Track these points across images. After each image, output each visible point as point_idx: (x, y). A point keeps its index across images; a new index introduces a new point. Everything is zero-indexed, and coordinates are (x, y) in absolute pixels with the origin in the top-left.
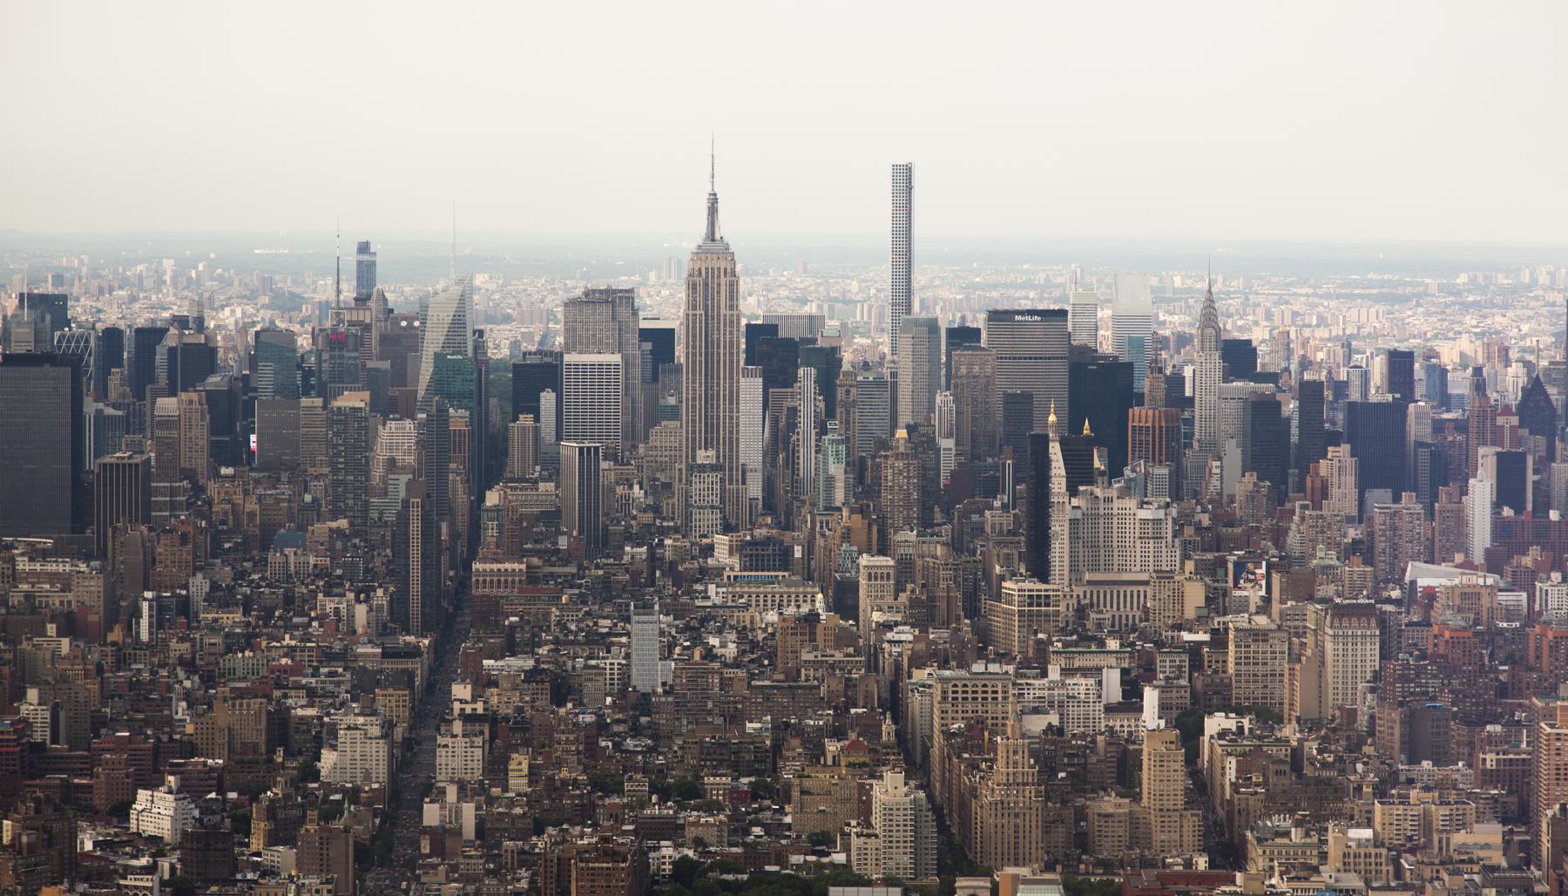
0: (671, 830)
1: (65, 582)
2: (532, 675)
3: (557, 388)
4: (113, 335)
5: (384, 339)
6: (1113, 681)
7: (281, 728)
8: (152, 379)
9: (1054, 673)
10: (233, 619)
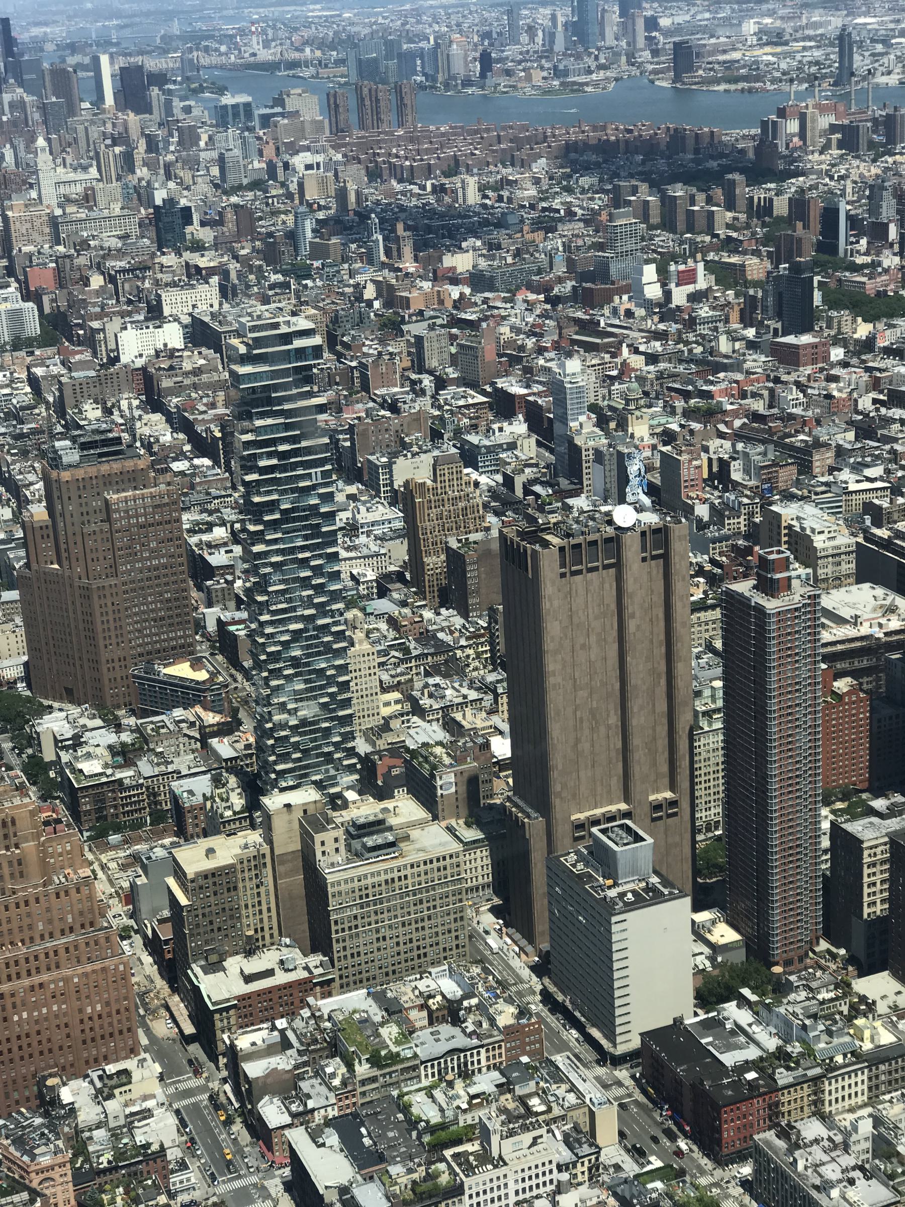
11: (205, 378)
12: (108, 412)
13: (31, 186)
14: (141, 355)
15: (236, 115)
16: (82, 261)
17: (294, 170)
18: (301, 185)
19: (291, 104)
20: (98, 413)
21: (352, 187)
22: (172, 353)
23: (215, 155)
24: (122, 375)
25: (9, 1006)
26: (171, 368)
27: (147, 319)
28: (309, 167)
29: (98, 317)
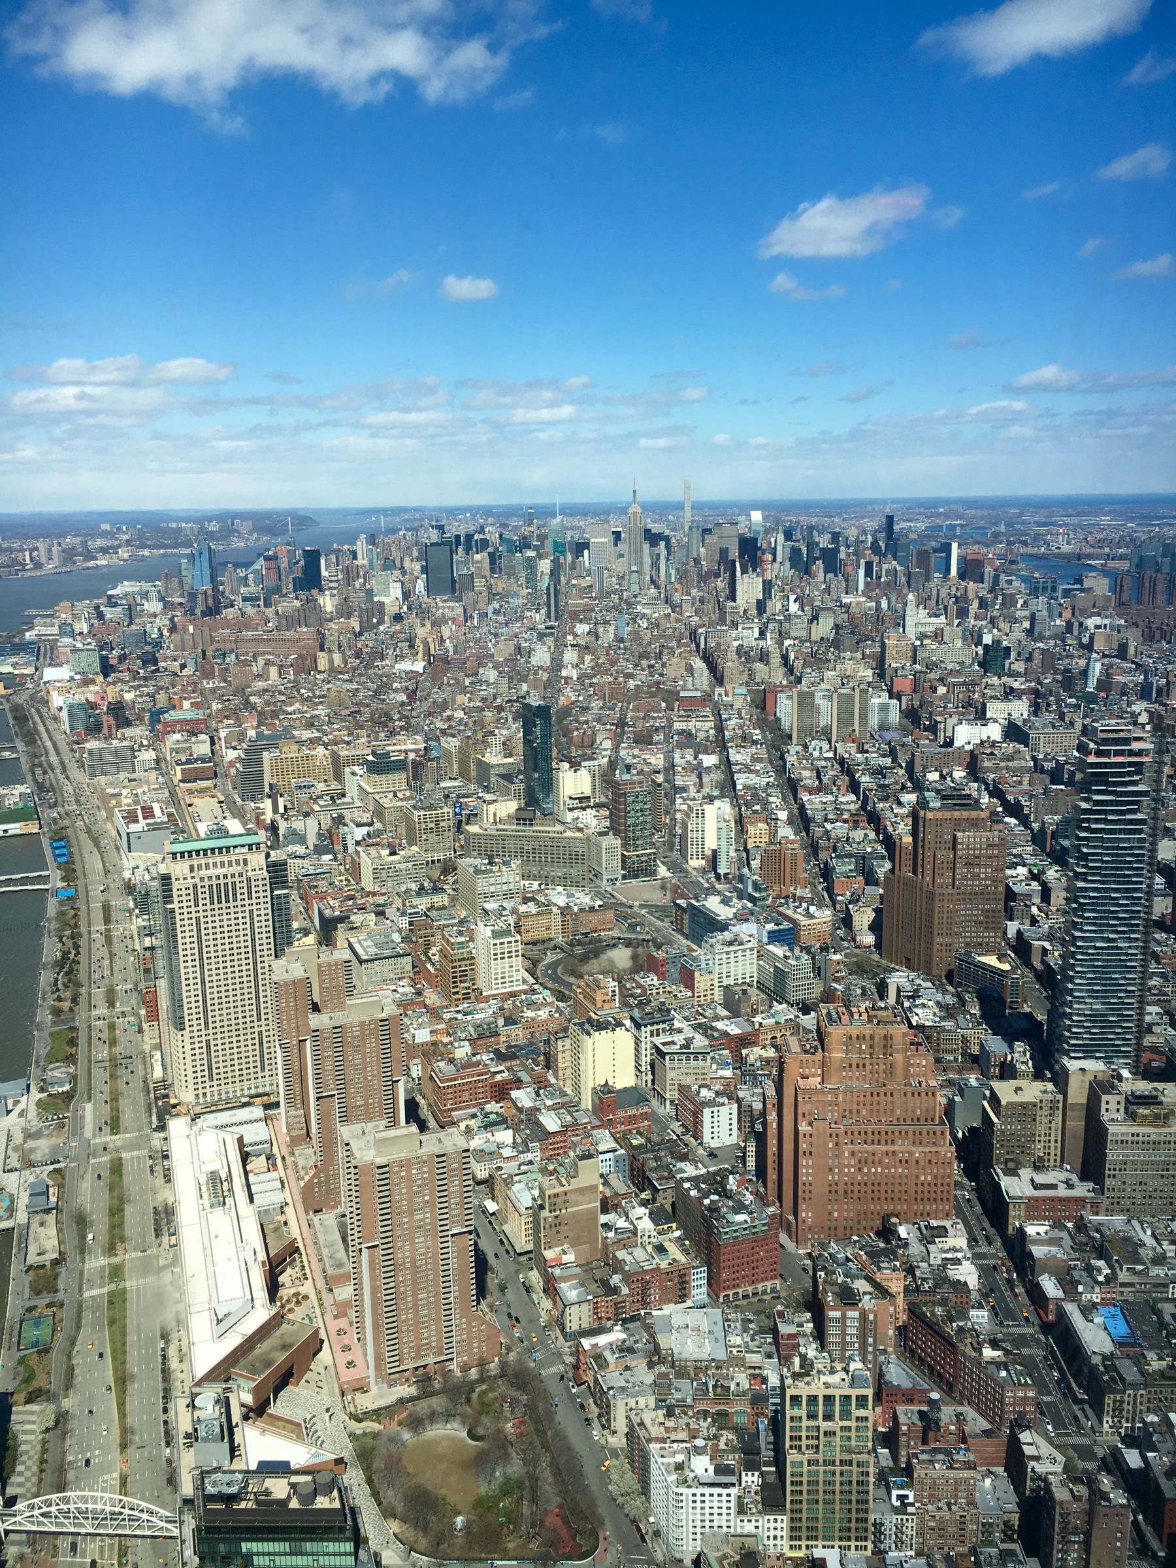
0: (631, 676)
1: (452, 608)
6: (756, 631)
7: (519, 649)
9: (740, 629)
10: (501, 618)
13: (899, 625)
15: (1045, 589)
16: (932, 676)
17: (1086, 628)
18: (1092, 638)
19: (1086, 585)
22: (993, 744)
23: (1027, 613)
24: (956, 755)
26: (992, 754)
27: (975, 719)
28: (1097, 627)
29: (940, 714)
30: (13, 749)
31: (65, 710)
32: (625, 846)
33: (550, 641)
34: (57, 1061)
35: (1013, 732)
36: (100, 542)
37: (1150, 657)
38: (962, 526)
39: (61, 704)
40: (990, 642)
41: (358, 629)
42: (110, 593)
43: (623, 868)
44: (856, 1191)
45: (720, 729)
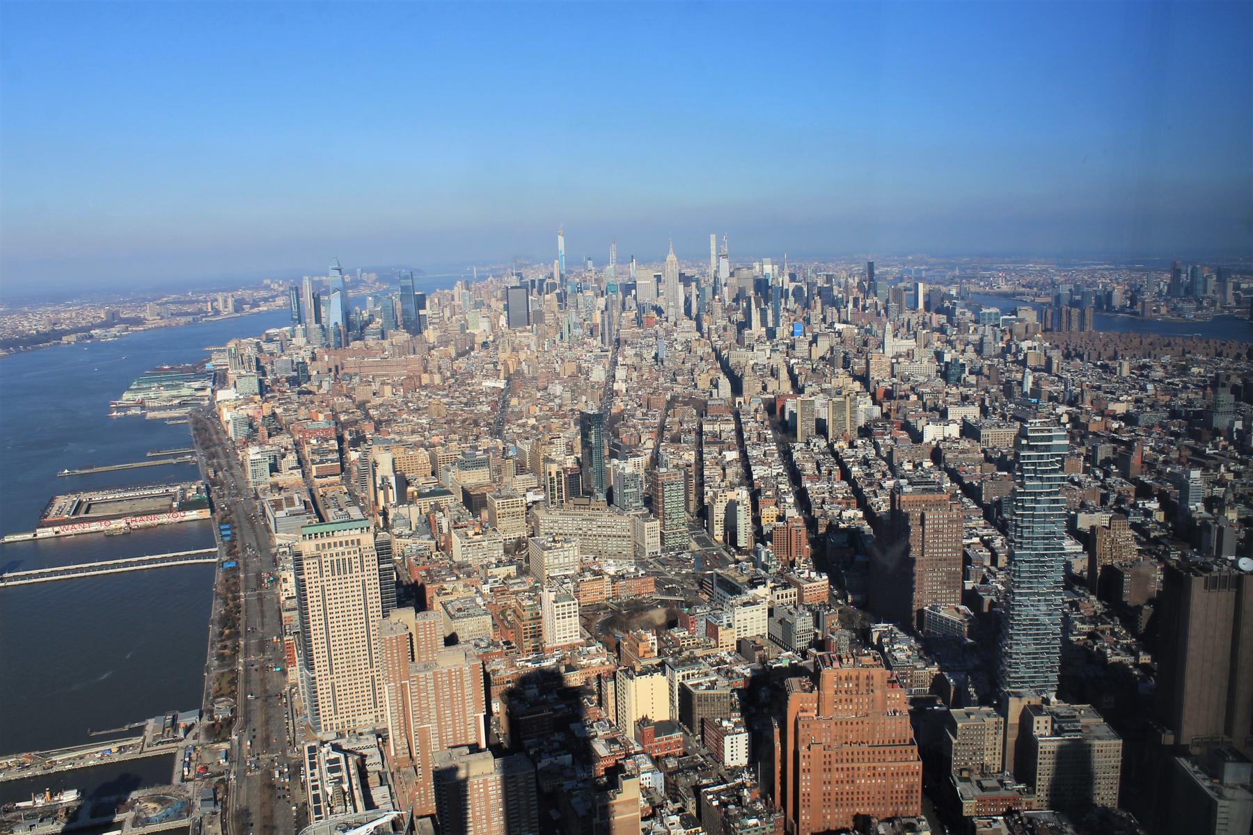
2: (636, 355)
3: (635, 288)
4: (533, 282)
5: (595, 279)
7: (579, 368)
8: (543, 291)
9: (755, 350)
11: (970, 455)
12: (915, 466)
14: (935, 439)
18: (1026, 355)
20: (911, 467)
21: (1055, 362)
22: (955, 441)
25: (856, 775)
27: (939, 420)
28: (1029, 348)
30: (193, 454)
31: (231, 422)
32: (663, 525)
33: (606, 362)
34: (222, 696)
35: (969, 431)
36: (263, 293)
37: (1068, 371)
38: (926, 270)
39: (229, 418)
40: (950, 360)
41: (454, 355)
42: (267, 332)
43: (662, 543)
44: (845, 799)
45: (739, 432)
